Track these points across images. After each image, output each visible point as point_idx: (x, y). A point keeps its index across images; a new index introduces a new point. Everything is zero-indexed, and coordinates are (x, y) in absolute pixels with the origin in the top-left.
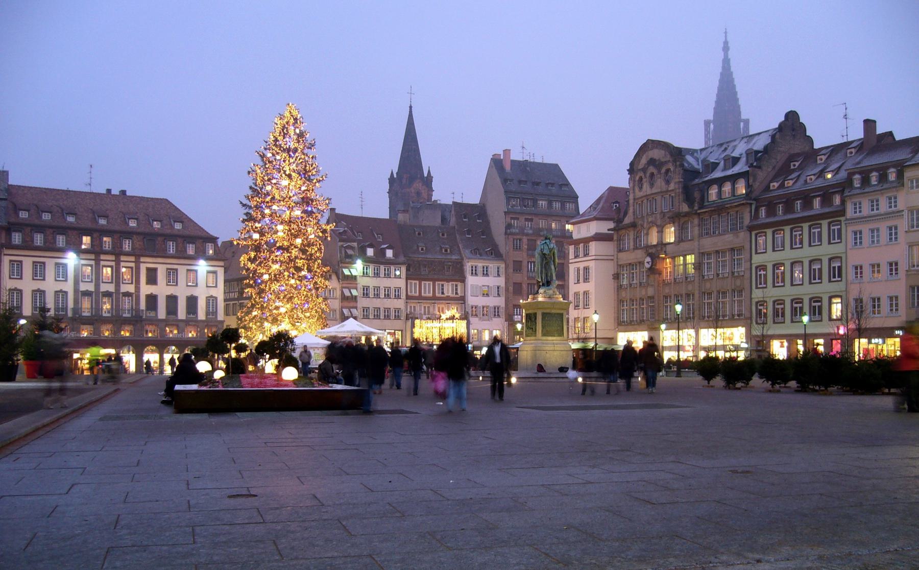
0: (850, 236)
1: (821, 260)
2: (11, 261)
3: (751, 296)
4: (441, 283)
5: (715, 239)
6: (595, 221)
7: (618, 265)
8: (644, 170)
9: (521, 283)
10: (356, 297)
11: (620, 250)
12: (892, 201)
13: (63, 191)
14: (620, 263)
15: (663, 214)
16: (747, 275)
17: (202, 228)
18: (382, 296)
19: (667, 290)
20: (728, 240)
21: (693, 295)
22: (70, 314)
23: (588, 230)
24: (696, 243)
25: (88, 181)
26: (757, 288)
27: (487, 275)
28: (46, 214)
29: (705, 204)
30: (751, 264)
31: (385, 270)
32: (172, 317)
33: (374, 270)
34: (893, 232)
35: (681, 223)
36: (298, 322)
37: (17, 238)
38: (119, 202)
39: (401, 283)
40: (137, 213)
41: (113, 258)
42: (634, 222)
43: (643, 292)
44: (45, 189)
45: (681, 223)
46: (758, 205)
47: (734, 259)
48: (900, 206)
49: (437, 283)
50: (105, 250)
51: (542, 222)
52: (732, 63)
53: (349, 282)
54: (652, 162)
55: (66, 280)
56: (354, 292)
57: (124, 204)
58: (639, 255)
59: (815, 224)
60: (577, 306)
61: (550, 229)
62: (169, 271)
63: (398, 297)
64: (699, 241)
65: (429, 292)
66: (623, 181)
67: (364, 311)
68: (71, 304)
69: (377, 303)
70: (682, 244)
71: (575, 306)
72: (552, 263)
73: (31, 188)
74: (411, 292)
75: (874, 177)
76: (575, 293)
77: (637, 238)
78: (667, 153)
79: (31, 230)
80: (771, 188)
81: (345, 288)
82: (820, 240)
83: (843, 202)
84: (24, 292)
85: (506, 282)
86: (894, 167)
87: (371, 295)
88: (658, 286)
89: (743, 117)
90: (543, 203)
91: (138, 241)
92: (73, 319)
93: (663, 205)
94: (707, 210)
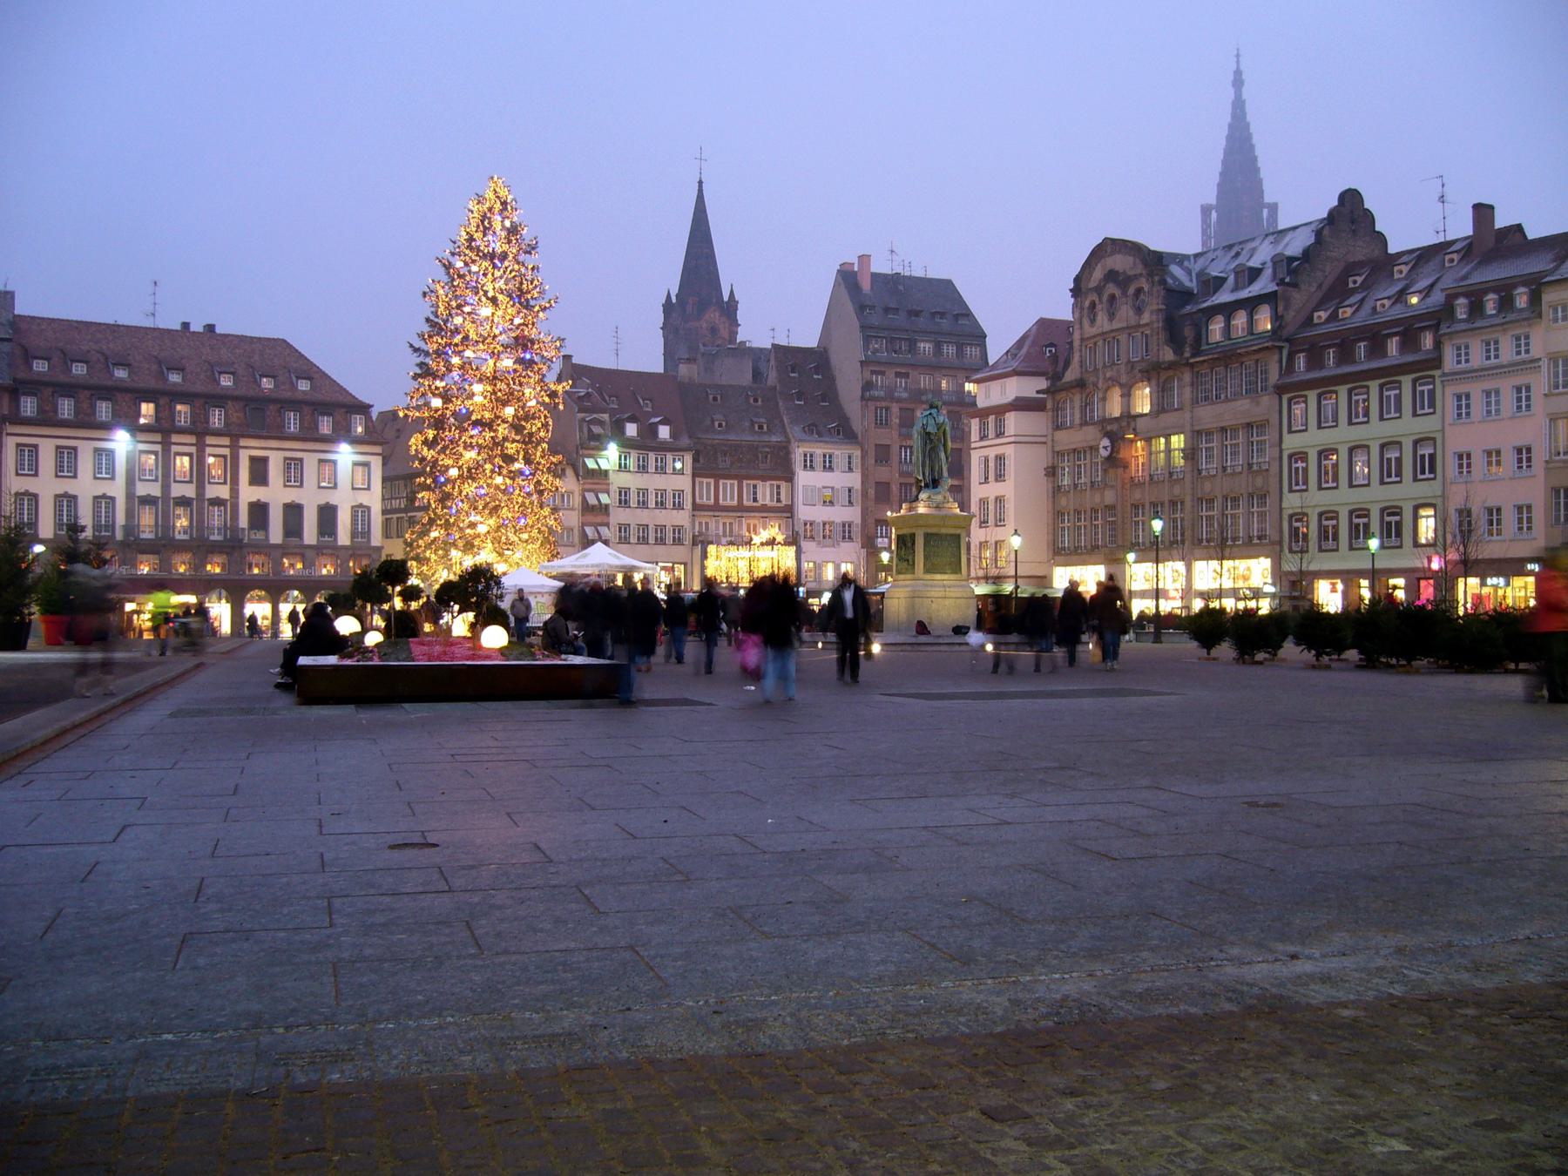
0: (1451, 403)
1: (1399, 443)
2: (18, 445)
3: (1281, 505)
4: (752, 482)
5: (1220, 408)
6: (1015, 378)
7: (1053, 452)
8: (1099, 290)
9: (889, 483)
10: (607, 506)
11: (1057, 428)
12: (1522, 342)
13: (108, 325)
14: (1057, 449)
15: (1131, 365)
16: (1274, 470)
17: (345, 389)
18: (652, 504)
19: (1137, 495)
20: (1241, 409)
21: (1182, 503)
22: (119, 535)
23: (1003, 392)
24: (1187, 415)
25: (150, 309)
26: (1291, 491)
27: (831, 469)
28: (79, 364)
29: (1203, 348)
30: (1281, 451)
31: (657, 461)
32: (294, 540)
33: (639, 460)
34: (1523, 395)
35: (1161, 381)
36: (508, 549)
37: (28, 406)
38: (202, 344)
39: (684, 483)
40: (233, 363)
41: (193, 439)
42: (1081, 379)
43: (1097, 499)
44: (77, 322)
45: (1161, 381)
46: (1294, 349)
47: (1252, 442)
48: (1536, 352)
49: (745, 482)
50: (180, 427)
51: (925, 378)
52: (1250, 109)
53: (596, 481)
54: (1112, 276)
55: (113, 478)
56: (604, 499)
57: (212, 349)
58: (1090, 434)
59: (1391, 382)
60: (984, 522)
61: (938, 391)
62: (288, 463)
63: (678, 506)
64: (1192, 412)
65: (732, 498)
66: (1063, 309)
67: (620, 531)
68: (121, 519)
69: (643, 517)
70: (1161, 416)
71: (981, 523)
72: (942, 448)
73: (53, 320)
74: (701, 498)
75: (1491, 303)
76: (980, 500)
77: (1086, 406)
78: (1138, 260)
79: (53, 393)
80: (1316, 321)
81: (589, 491)
82: (1399, 409)
83: (1438, 345)
84: (40, 498)
85: (862, 482)
86: (1524, 284)
87: (633, 503)
88: (1123, 487)
89: (1268, 199)
90: (925, 347)
91: (236, 411)
92: (125, 544)
93: (1131, 350)
94: (1206, 358)
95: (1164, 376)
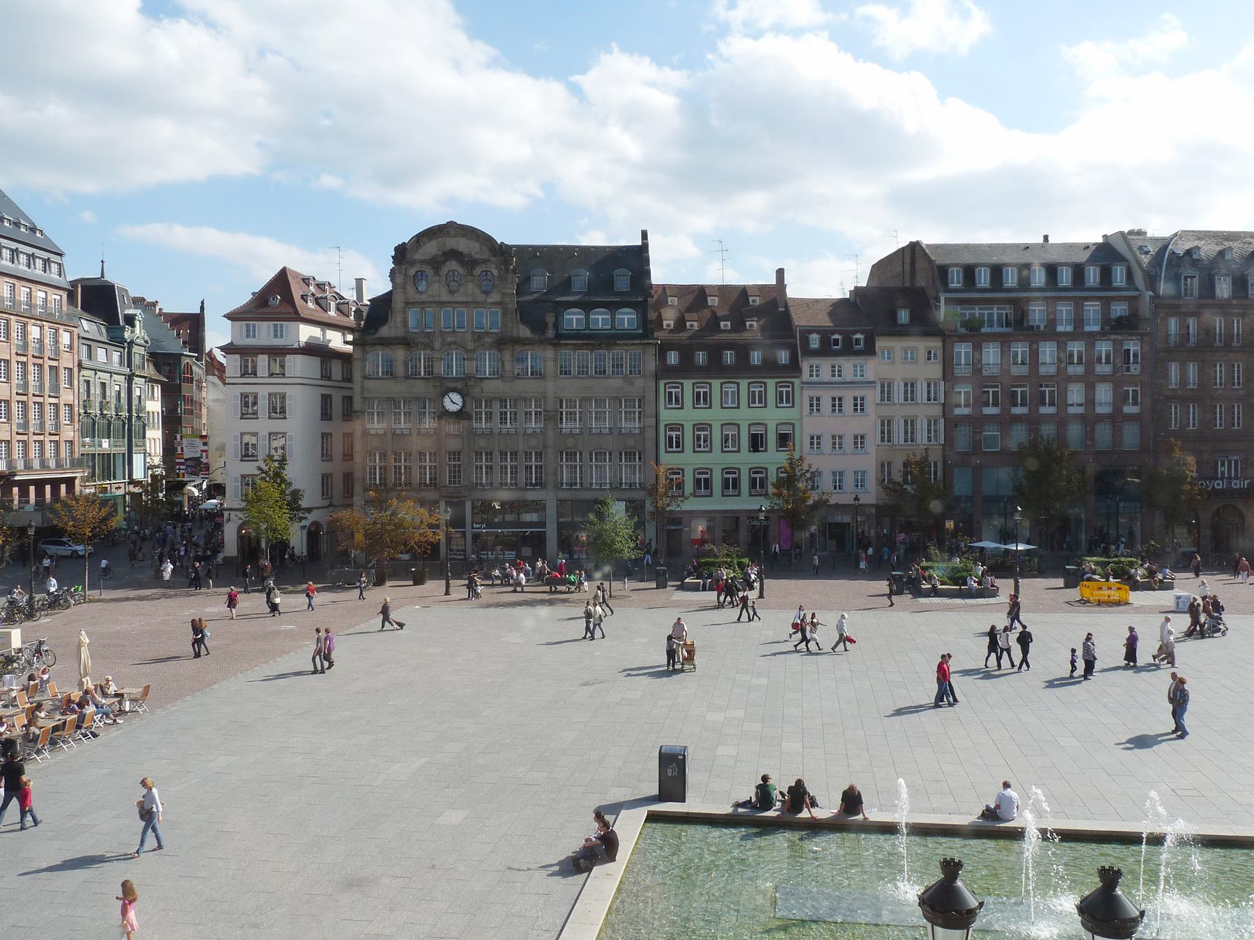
8: (436, 263)
11: (365, 378)
16: (650, 434)
26: (666, 452)
34: (859, 405)
48: (870, 376)
54: (454, 254)
71: (242, 456)
78: (484, 248)
80: (665, 327)
95: (518, 348)
